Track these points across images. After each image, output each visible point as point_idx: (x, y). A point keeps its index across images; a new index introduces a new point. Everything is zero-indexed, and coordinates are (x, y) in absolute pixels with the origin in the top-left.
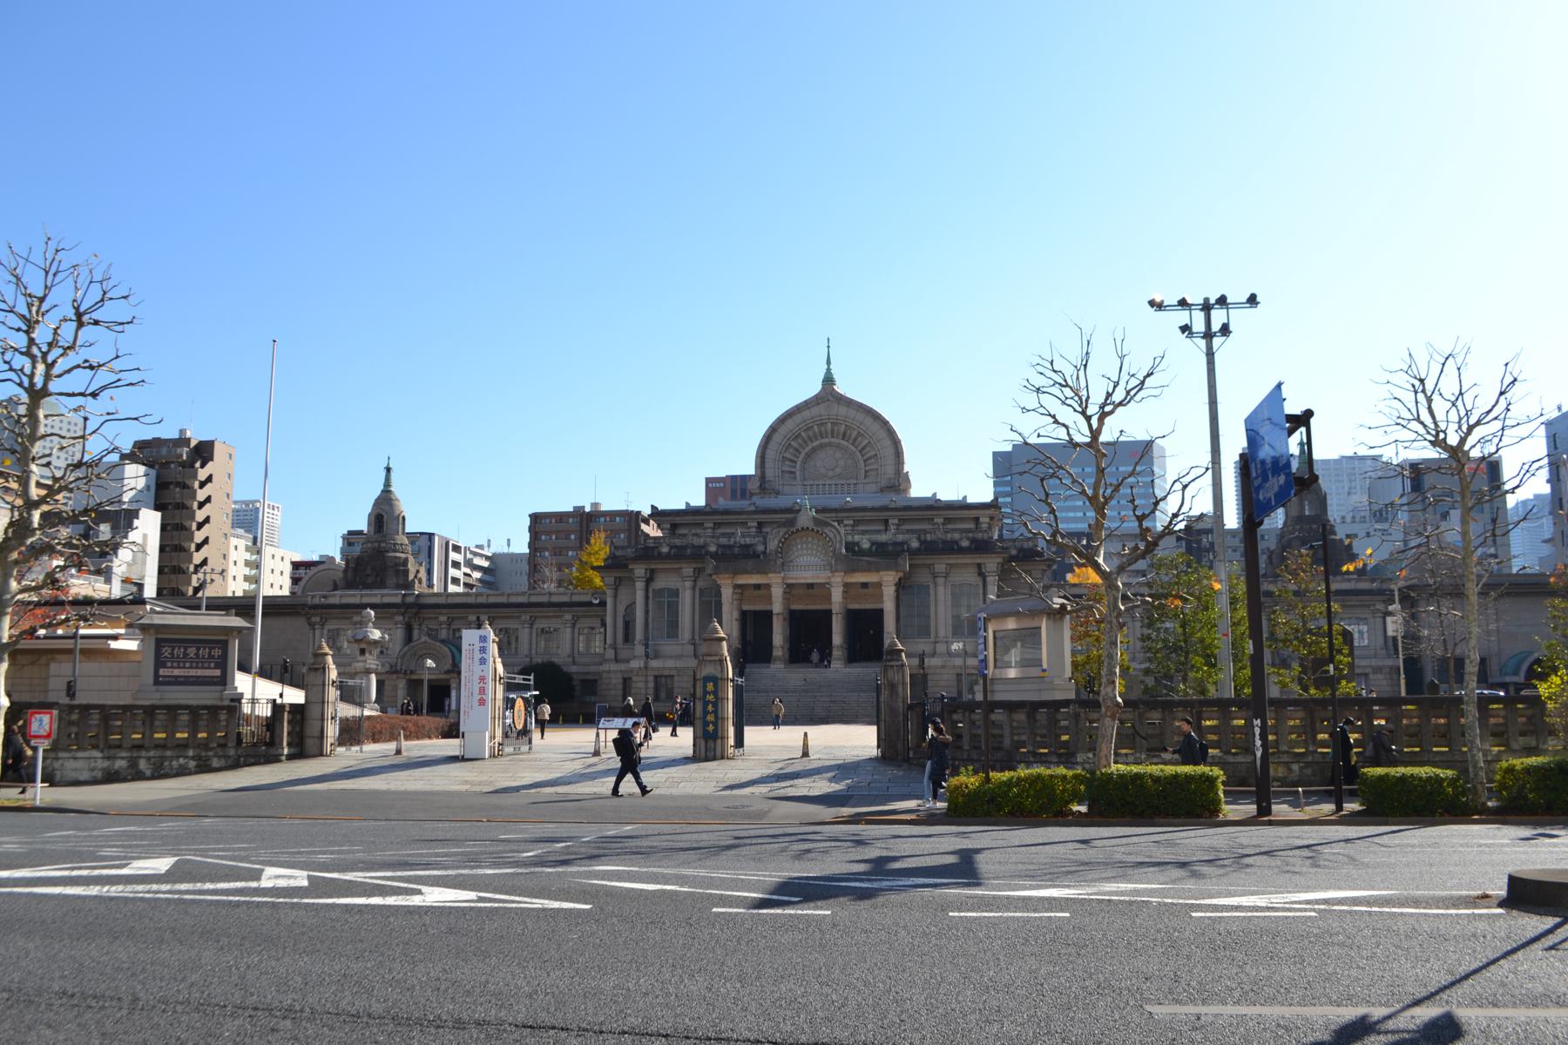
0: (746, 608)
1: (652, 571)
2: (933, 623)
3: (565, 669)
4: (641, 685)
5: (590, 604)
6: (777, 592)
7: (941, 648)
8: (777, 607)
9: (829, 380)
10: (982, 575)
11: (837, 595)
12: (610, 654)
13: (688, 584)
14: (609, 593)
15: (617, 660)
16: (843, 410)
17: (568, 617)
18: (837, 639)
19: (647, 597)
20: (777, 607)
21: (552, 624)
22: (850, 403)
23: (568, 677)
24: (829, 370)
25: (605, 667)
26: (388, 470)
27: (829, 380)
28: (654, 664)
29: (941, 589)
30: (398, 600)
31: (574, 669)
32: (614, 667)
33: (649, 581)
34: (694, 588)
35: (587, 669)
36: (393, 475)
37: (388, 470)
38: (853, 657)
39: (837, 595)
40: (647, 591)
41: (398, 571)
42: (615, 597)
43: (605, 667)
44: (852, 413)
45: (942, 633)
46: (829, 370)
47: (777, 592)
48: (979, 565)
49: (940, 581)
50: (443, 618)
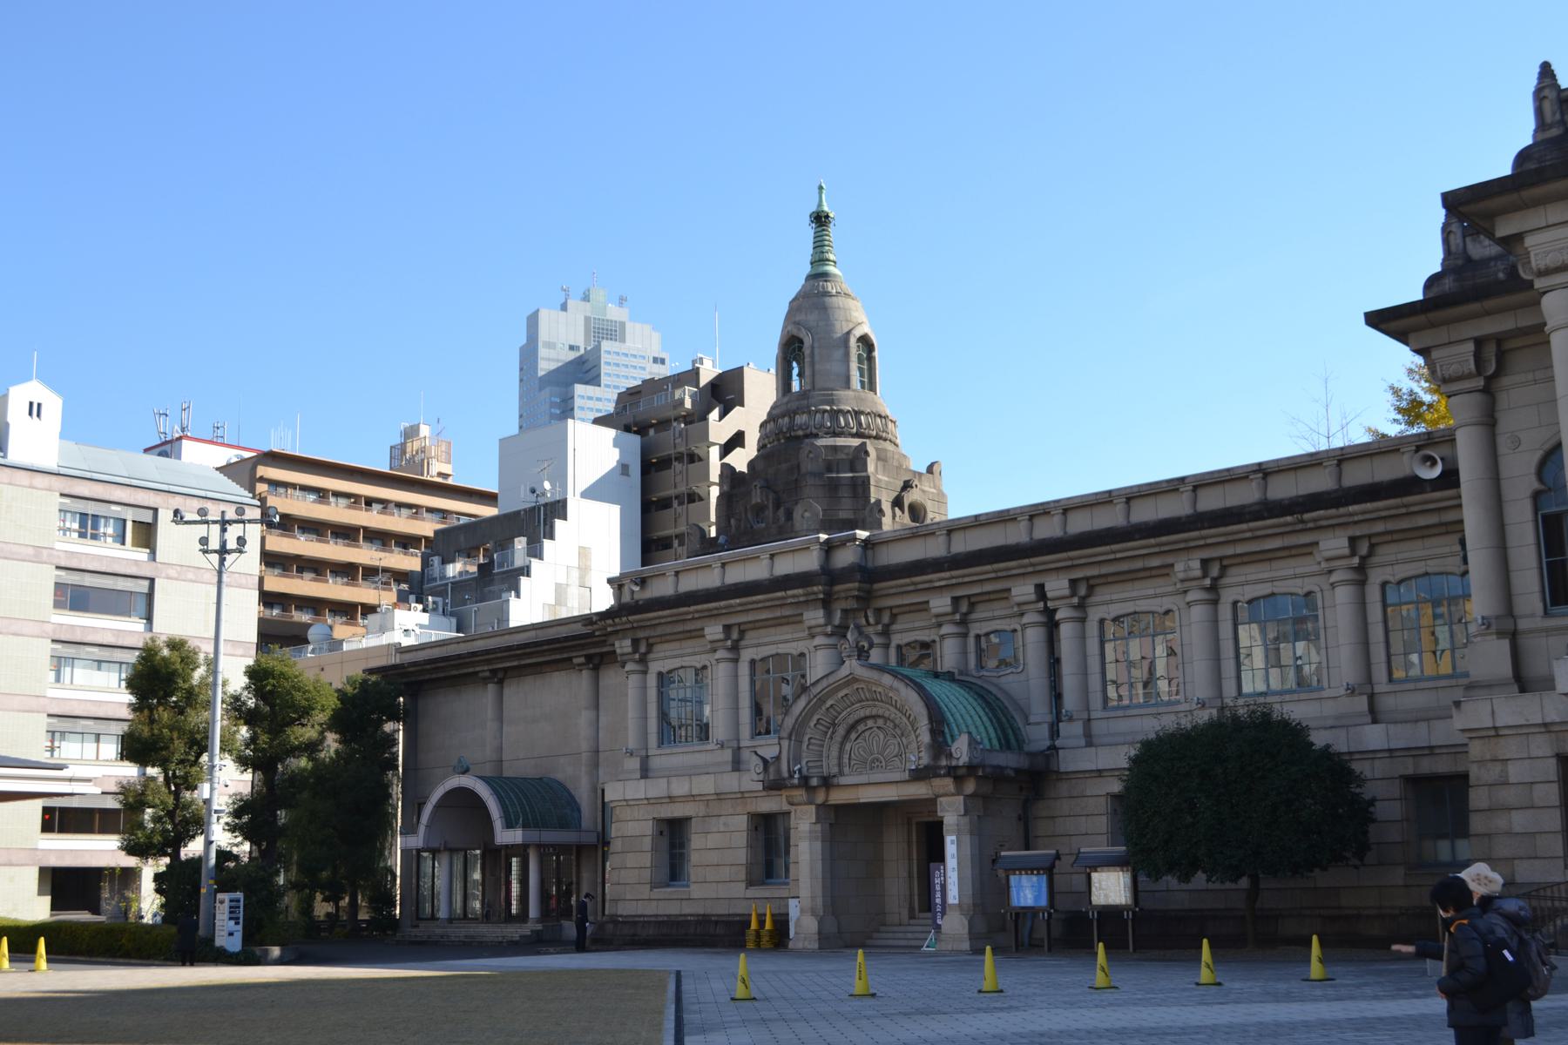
3: (1319, 739)
5: (1411, 485)
12: (1492, 658)
14: (1468, 406)
15: (1523, 681)
21: (1291, 577)
23: (1335, 770)
25: (1477, 714)
26: (820, 220)
30: (809, 562)
31: (1375, 737)
32: (1511, 710)
35: (1419, 735)
36: (833, 232)
37: (820, 220)
41: (833, 487)
42: (1489, 422)
43: (1477, 714)
50: (940, 604)
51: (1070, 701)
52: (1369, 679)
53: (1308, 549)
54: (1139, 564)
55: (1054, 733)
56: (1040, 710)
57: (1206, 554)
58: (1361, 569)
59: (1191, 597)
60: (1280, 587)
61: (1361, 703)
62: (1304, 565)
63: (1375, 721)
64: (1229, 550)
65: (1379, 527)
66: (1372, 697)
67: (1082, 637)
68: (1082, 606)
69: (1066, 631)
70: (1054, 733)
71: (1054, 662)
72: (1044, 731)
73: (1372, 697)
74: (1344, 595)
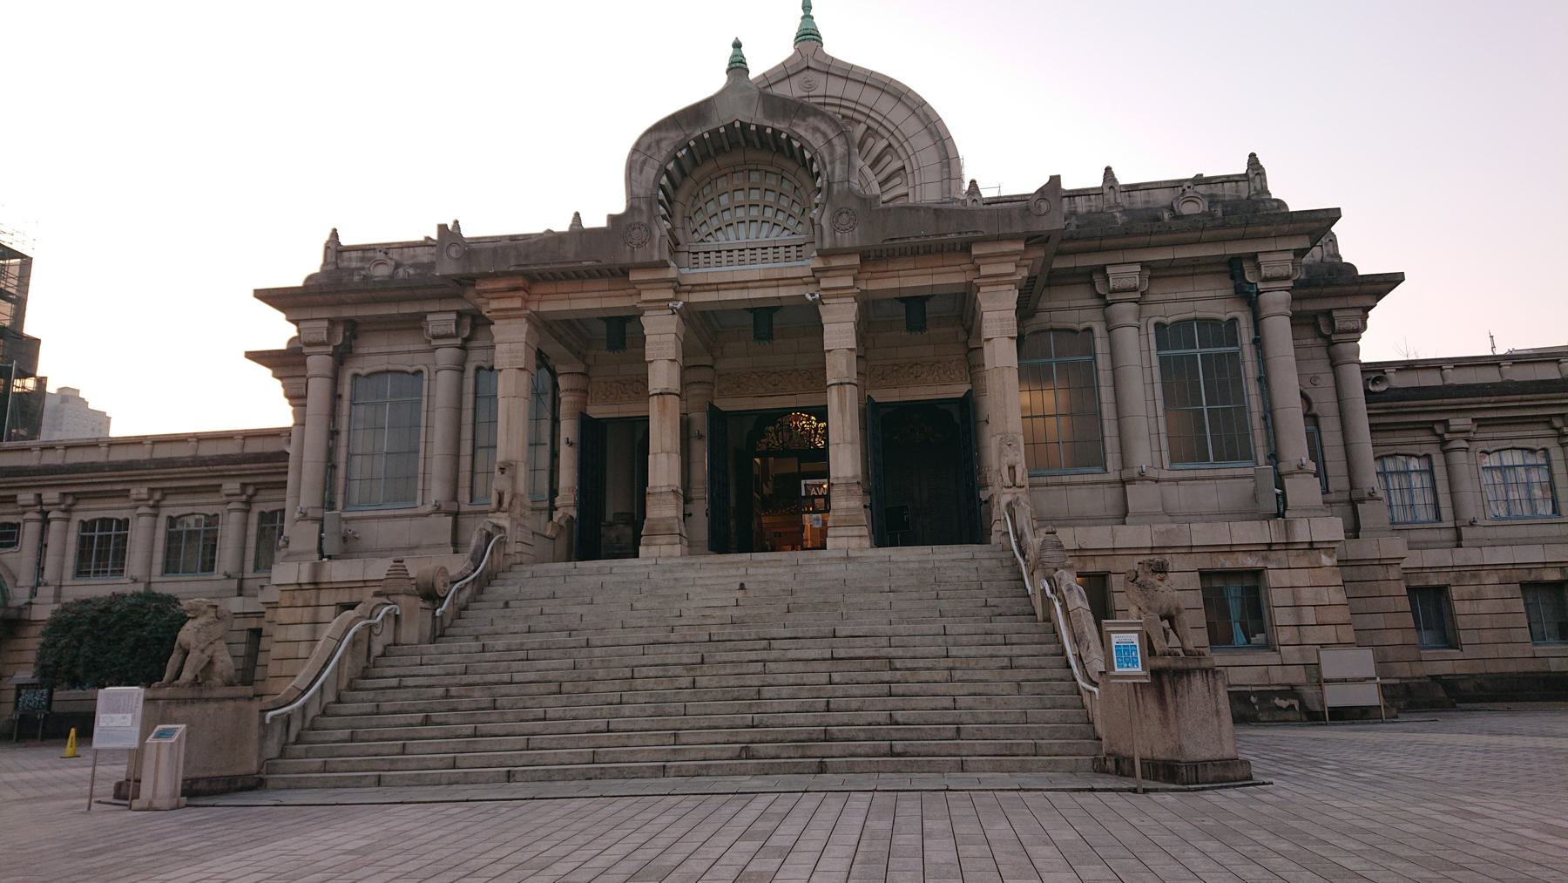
0: (597, 411)
1: (354, 329)
2: (1110, 429)
4: (302, 632)
6: (662, 338)
7: (1138, 496)
8: (663, 374)
9: (808, 36)
10: (1249, 297)
11: (840, 331)
13: (446, 355)
16: (836, 87)
17: (231, 486)
18: (845, 461)
19: (336, 397)
20: (663, 374)
22: (848, 74)
24: (807, 17)
27: (808, 36)
28: (337, 571)
29: (1130, 340)
33: (341, 357)
34: (460, 368)
38: (892, 525)
39: (840, 331)
40: (335, 379)
44: (853, 91)
45: (1144, 456)
46: (807, 17)
47: (662, 338)
48: (1233, 267)
49: (1125, 311)
51: (49, 574)
52: (242, 570)
53: (216, 489)
54: (108, 488)
55: (34, 593)
56: (26, 578)
57: (152, 485)
58: (248, 502)
59: (140, 510)
60: (197, 509)
61: (234, 584)
62: (215, 498)
63: (240, 595)
64: (167, 484)
65: (261, 479)
66: (241, 581)
67: (66, 531)
68: (68, 511)
69: (54, 525)
70: (34, 593)
71: (42, 546)
72: (27, 592)
73: (241, 581)
74: (235, 517)
